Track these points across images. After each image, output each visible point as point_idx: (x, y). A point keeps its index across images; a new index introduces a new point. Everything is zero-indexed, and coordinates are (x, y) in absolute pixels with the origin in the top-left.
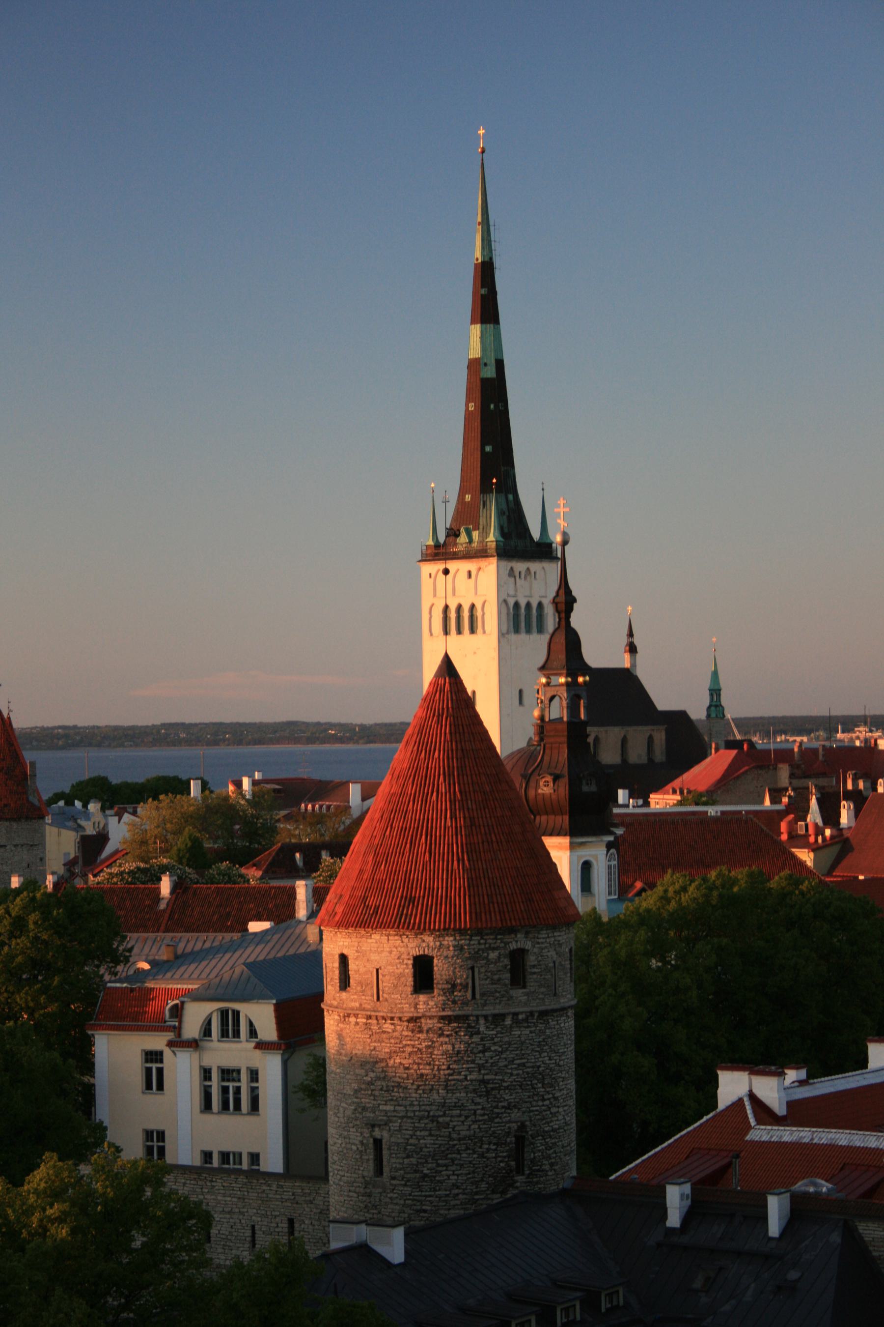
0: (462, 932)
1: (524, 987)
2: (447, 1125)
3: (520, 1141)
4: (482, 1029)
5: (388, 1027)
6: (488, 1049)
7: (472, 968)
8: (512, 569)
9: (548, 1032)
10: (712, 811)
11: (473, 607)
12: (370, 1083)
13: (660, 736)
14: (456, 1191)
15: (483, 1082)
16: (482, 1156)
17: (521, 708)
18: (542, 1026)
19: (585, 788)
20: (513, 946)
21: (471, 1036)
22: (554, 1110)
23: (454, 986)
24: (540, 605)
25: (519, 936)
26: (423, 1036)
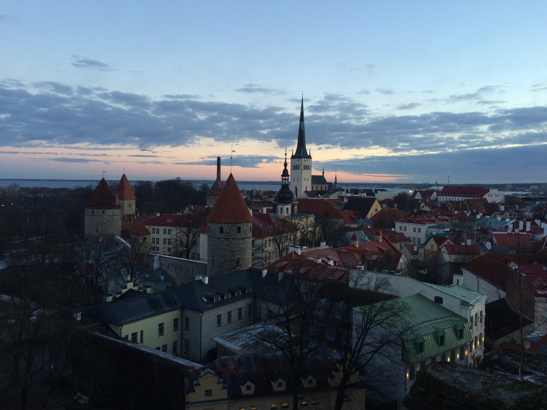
0: (228, 223)
1: (240, 233)
2: (225, 257)
3: (238, 261)
4: (232, 241)
5: (215, 239)
6: (233, 244)
7: (230, 230)
8: (304, 160)
9: (244, 241)
10: (326, 199)
11: (298, 165)
12: (212, 249)
13: (327, 186)
14: (226, 269)
15: (231, 250)
16: (231, 263)
17: (305, 181)
18: (243, 240)
19: (288, 196)
20: (238, 226)
21: (230, 241)
22: (245, 255)
23: (227, 233)
24: (309, 165)
25: (239, 224)
26: (221, 241)
